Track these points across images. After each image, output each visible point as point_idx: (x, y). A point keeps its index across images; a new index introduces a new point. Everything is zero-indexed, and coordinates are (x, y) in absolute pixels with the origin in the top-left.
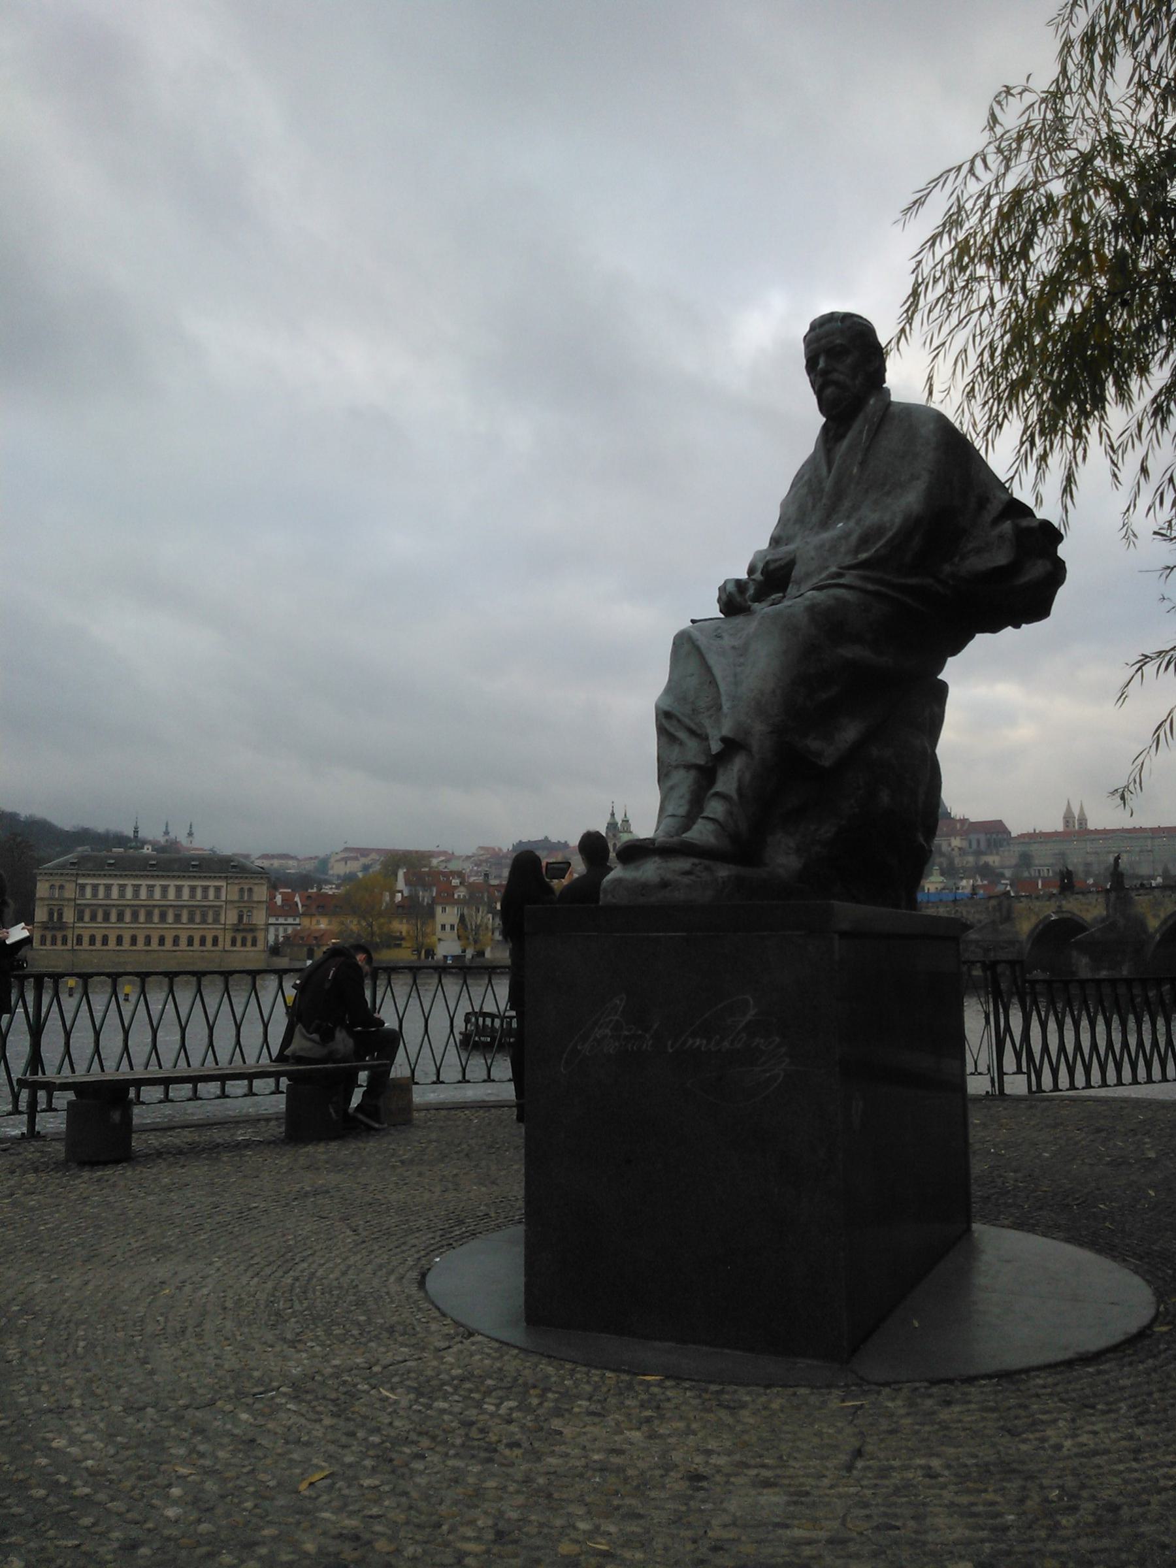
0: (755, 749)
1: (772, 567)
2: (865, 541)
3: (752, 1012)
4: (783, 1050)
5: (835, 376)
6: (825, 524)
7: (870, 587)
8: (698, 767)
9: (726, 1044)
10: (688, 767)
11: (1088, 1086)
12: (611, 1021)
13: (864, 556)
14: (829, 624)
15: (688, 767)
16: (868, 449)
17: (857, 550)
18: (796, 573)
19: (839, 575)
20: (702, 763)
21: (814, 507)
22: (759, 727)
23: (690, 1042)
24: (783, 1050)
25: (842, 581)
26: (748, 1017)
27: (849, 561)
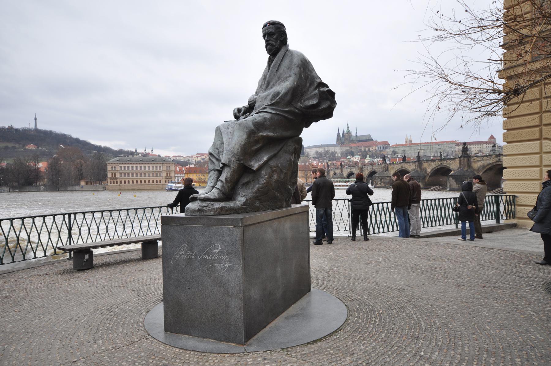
2: (274, 97)
5: (270, 42)
6: (266, 90)
7: (274, 112)
11: (379, 232)
14: (259, 126)
16: (279, 66)
17: (272, 100)
19: (265, 108)
22: (233, 159)
27: (269, 103)
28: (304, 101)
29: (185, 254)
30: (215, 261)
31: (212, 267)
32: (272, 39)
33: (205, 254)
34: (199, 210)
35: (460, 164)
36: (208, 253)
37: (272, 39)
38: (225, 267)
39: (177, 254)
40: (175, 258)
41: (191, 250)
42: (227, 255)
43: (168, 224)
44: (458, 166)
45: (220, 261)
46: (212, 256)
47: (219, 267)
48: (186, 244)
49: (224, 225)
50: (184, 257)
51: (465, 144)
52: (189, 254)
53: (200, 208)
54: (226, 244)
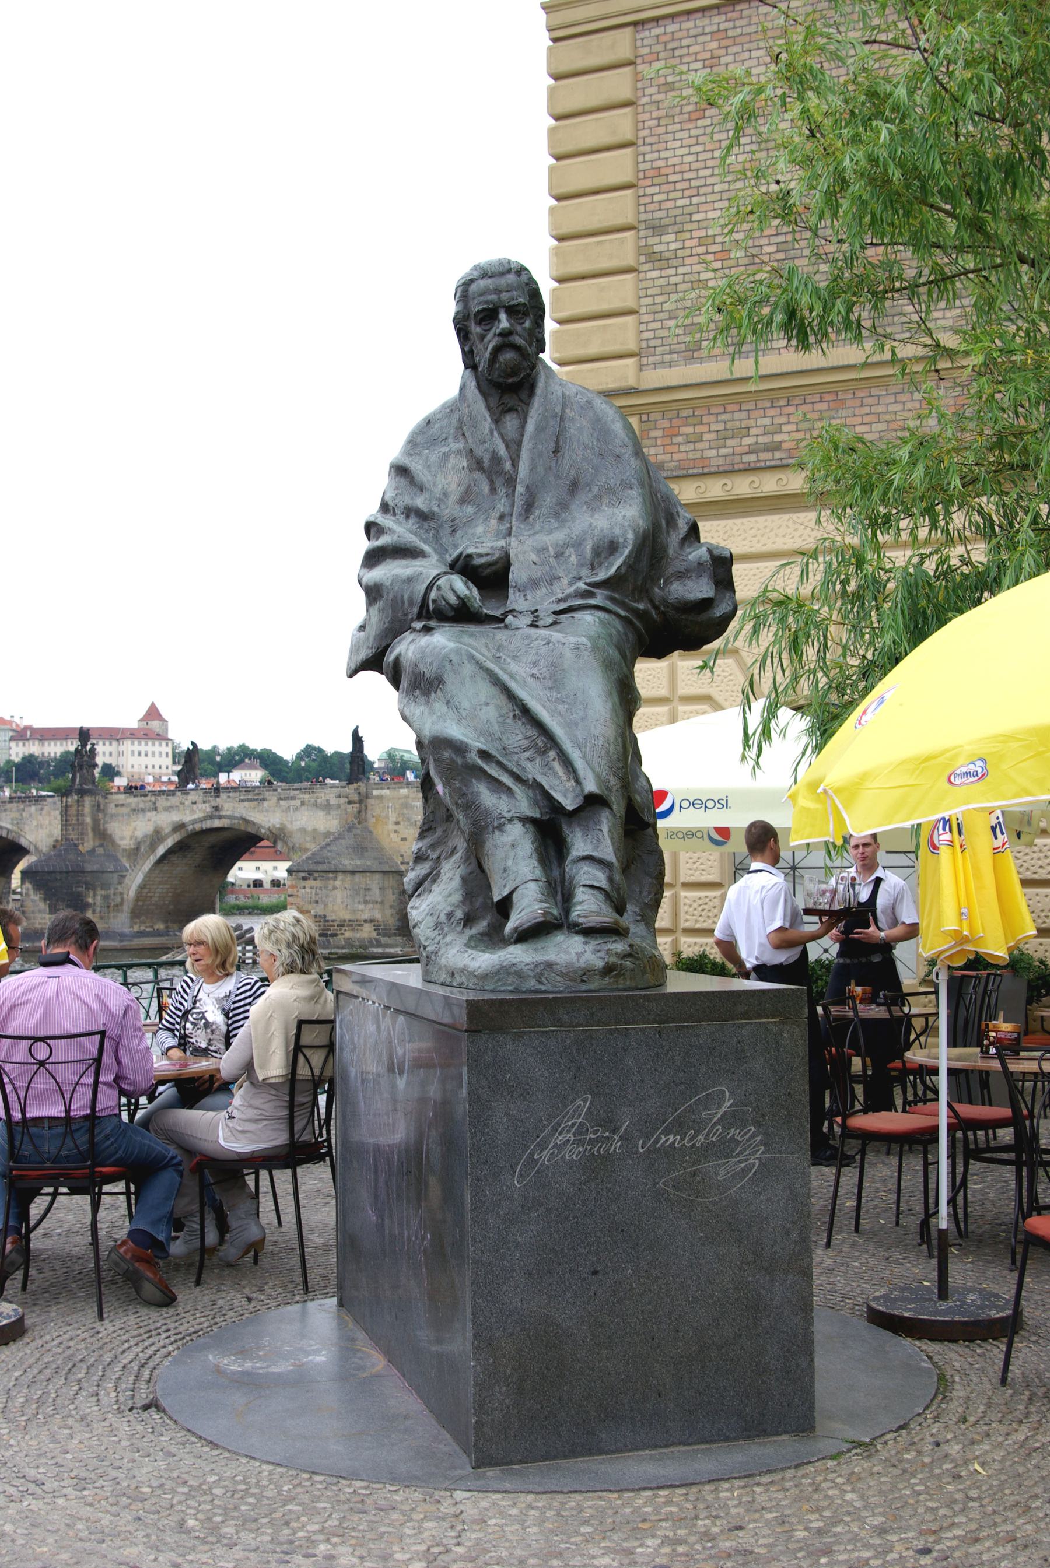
0: (614, 807)
1: (477, 561)
3: (728, 1104)
4: (758, 1139)
5: (519, 341)
7: (623, 613)
8: (533, 821)
9: (701, 1138)
10: (525, 820)
12: (574, 1124)
13: (602, 575)
15: (525, 820)
18: (517, 574)
20: (538, 815)
21: (493, 490)
23: (664, 1139)
24: (758, 1139)
25: (592, 602)
26: (723, 1109)
28: (668, 582)
29: (579, 1143)
30: (707, 1151)
31: (694, 1174)
32: (519, 328)
33: (667, 1132)
34: (608, 970)
35: (66, 824)
36: (680, 1126)
37: (519, 328)
38: (747, 1169)
39: (542, 1146)
40: (532, 1161)
41: (609, 1123)
42: (758, 1124)
43: (501, 1030)
44: (57, 832)
45: (725, 1148)
46: (698, 1133)
47: (721, 1170)
48: (584, 1103)
49: (745, 1015)
50: (574, 1154)
51: (84, 735)
52: (598, 1140)
53: (613, 959)
54: (751, 1086)
